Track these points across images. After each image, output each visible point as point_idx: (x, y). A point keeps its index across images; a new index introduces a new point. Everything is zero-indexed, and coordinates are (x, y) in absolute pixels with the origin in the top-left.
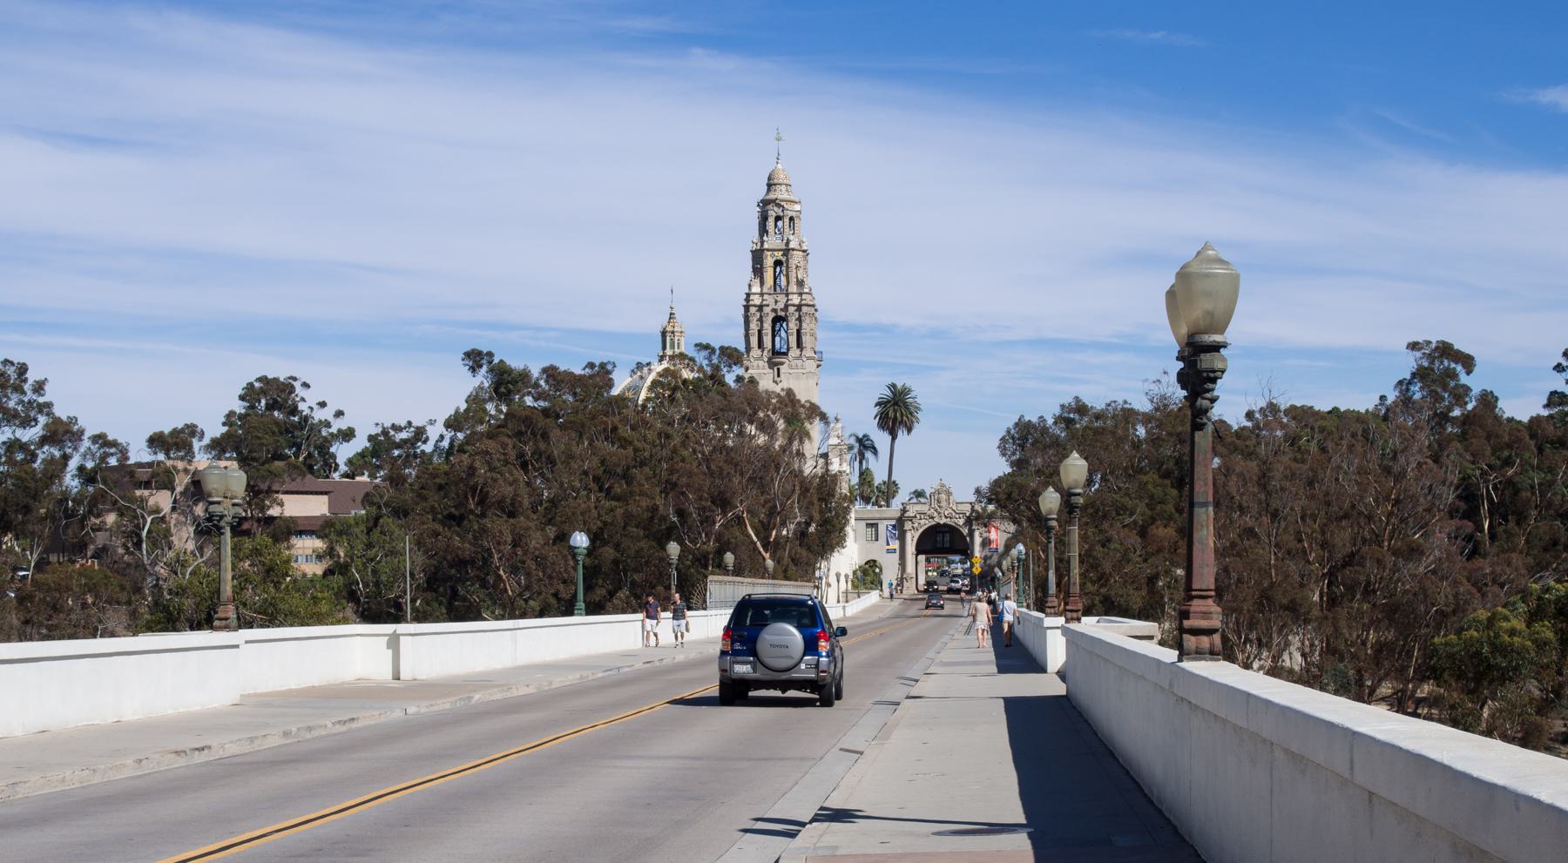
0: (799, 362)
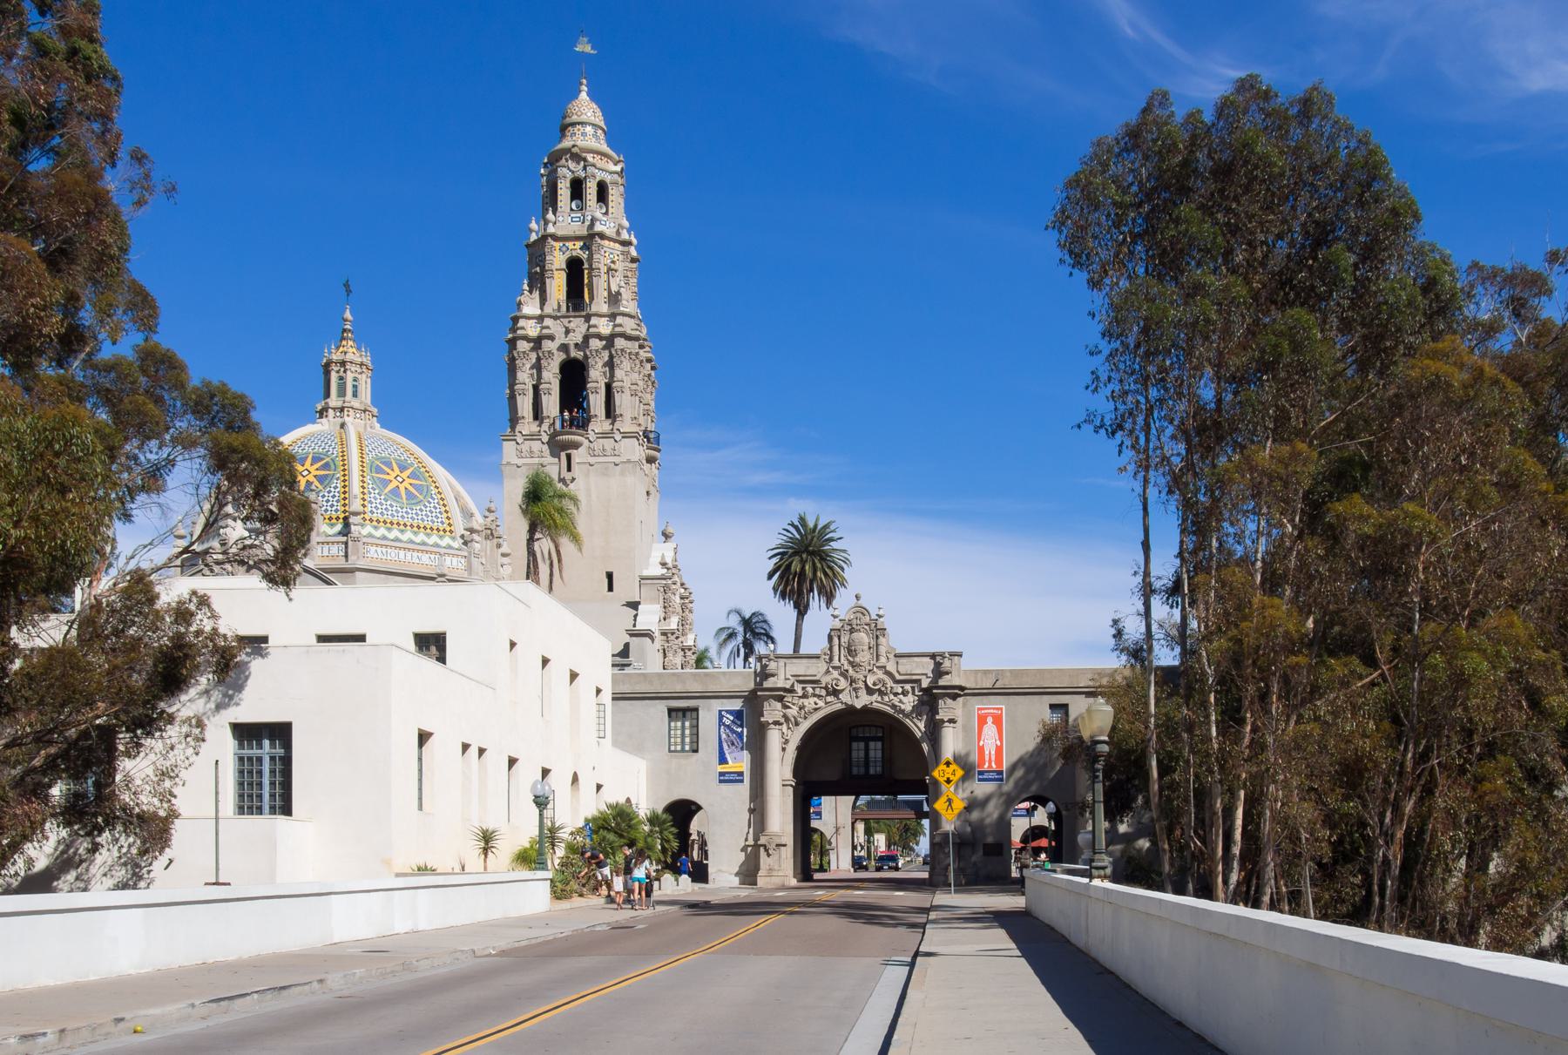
0: (608, 443)
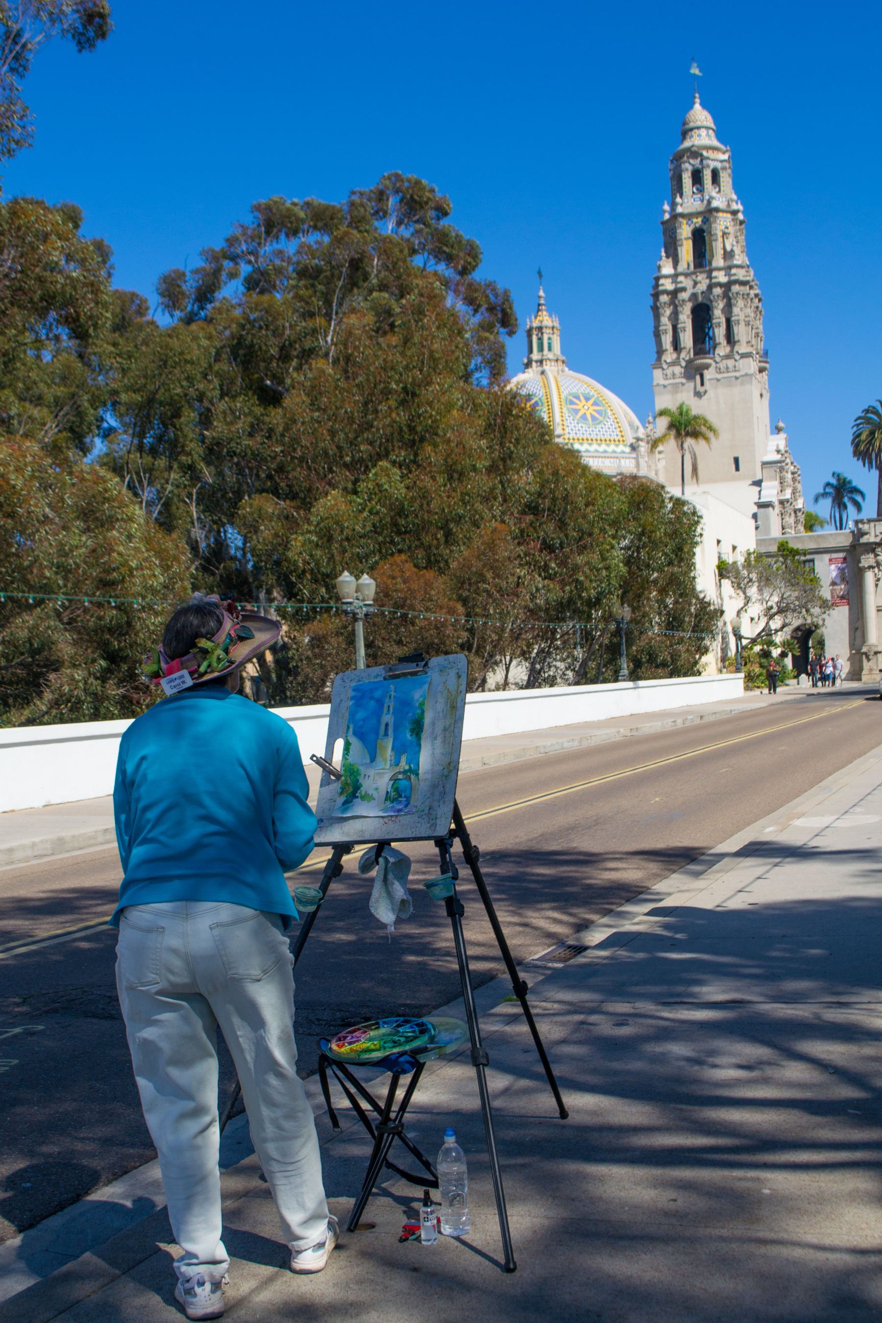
0: (730, 363)
